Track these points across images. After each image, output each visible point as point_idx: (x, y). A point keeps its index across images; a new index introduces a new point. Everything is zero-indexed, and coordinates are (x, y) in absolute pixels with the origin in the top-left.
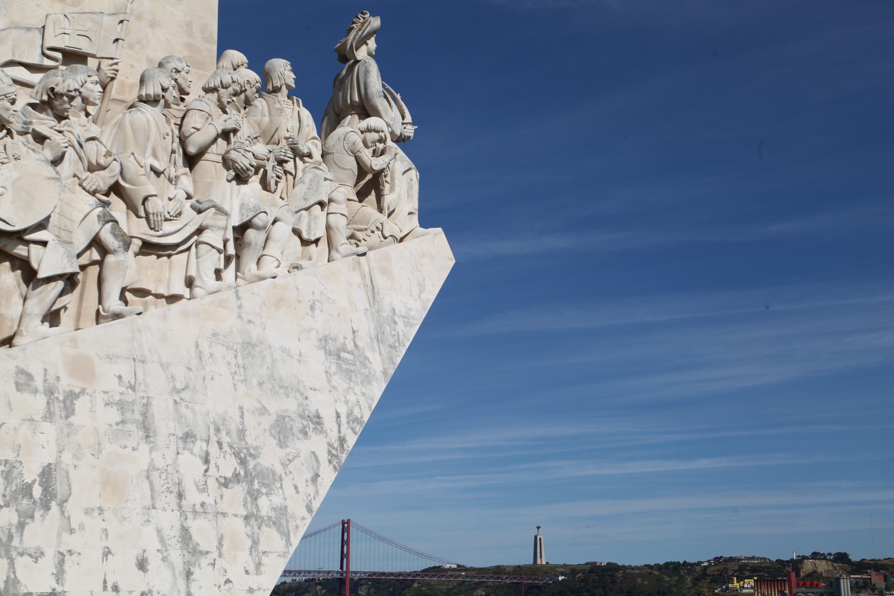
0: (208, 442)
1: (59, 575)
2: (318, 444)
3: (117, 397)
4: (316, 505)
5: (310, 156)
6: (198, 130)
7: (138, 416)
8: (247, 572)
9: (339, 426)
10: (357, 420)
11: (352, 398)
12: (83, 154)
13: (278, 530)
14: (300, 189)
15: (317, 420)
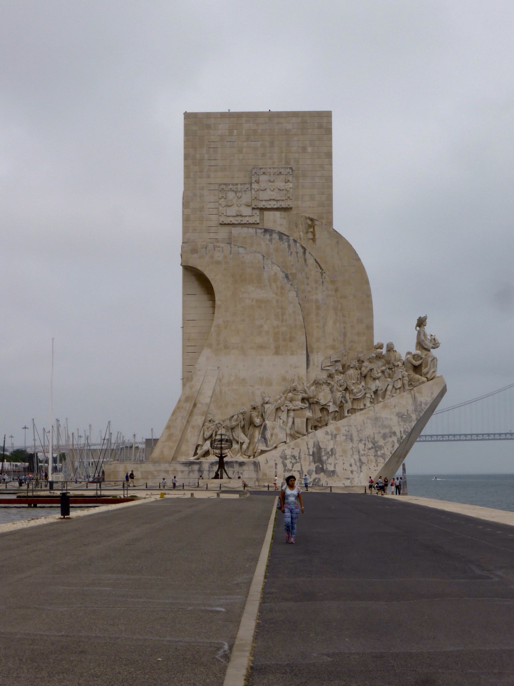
0: (365, 441)
1: (335, 467)
2: (395, 439)
3: (345, 434)
4: (393, 452)
5: (398, 365)
6: (364, 371)
7: (349, 437)
8: (374, 467)
9: (401, 434)
10: (407, 432)
11: (405, 427)
12: (338, 384)
13: (383, 458)
14: (395, 375)
15: (395, 433)
